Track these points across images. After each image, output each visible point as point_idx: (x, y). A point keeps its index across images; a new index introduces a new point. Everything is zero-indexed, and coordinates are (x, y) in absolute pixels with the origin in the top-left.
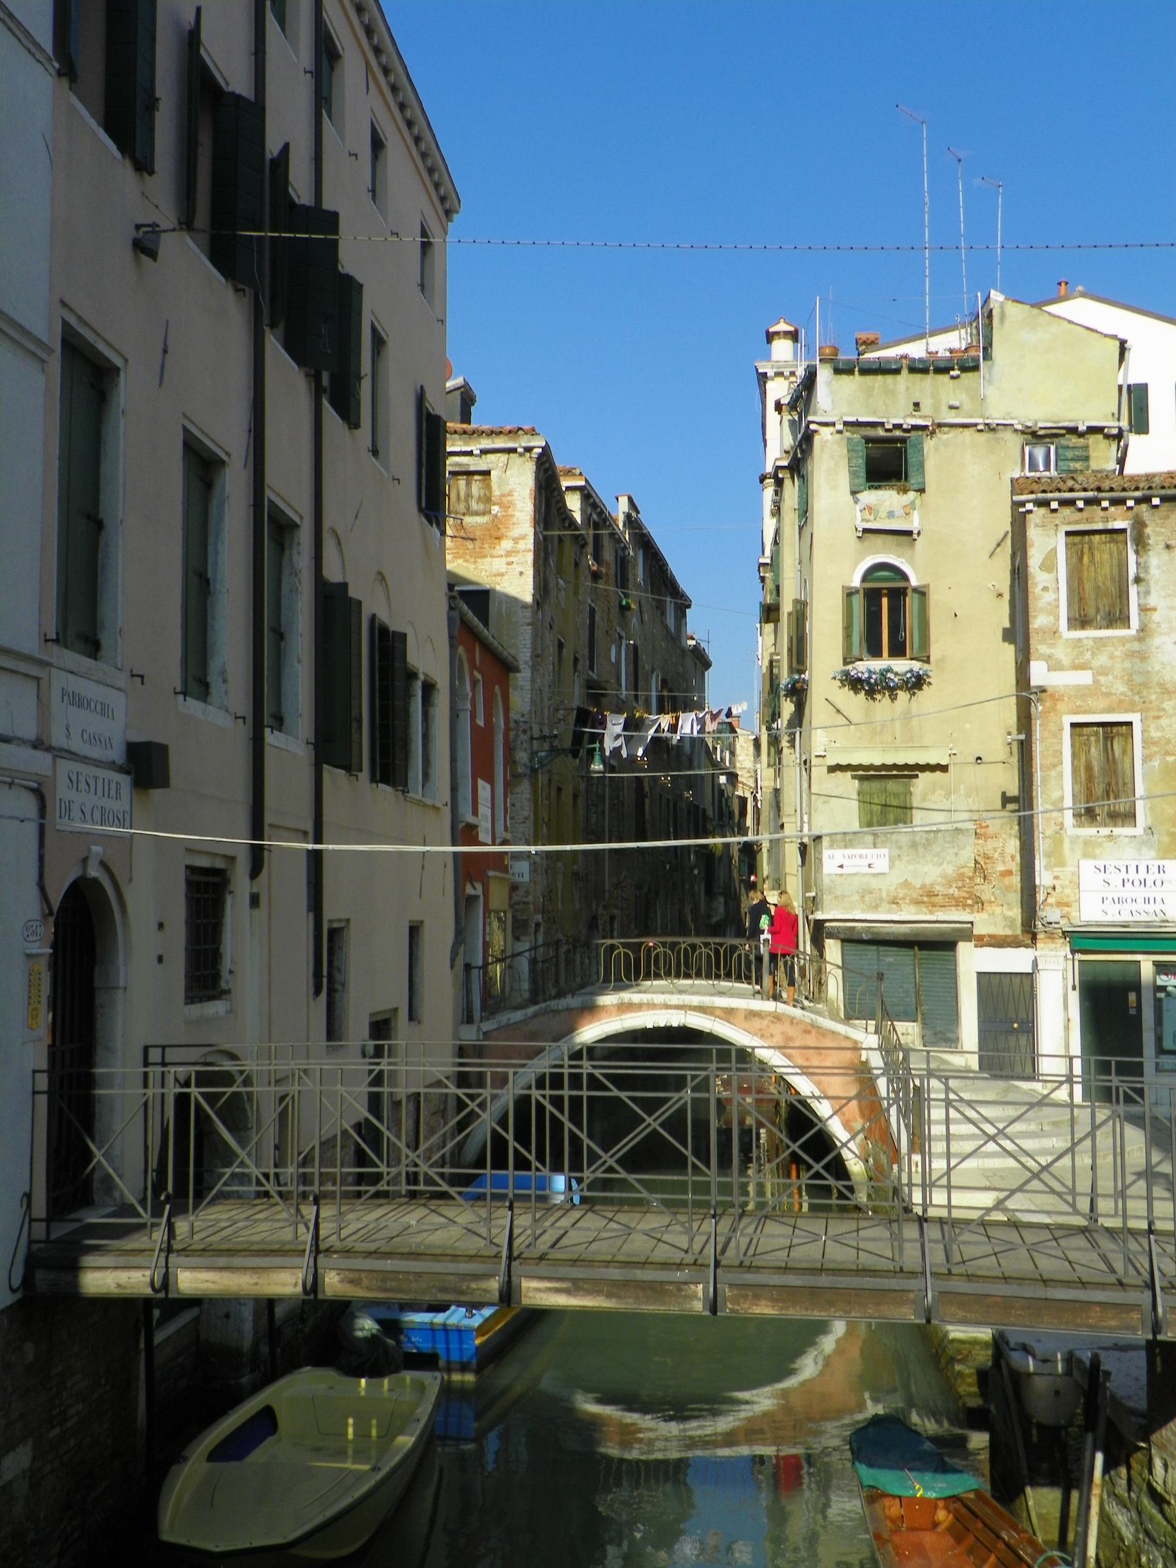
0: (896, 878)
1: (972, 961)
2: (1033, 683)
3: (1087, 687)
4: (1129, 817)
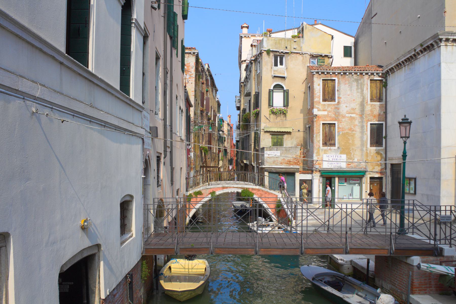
1: (299, 177)
2: (314, 114)
4: (334, 145)
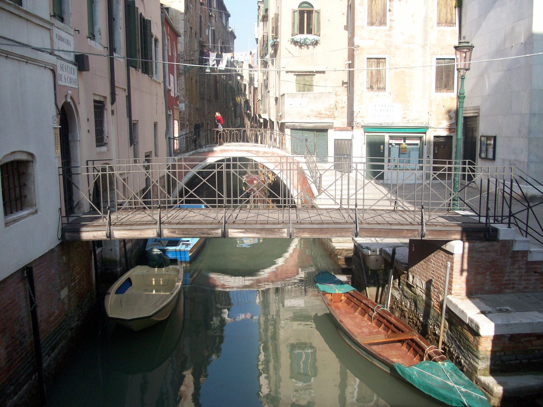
1: (332, 135)
2: (355, 44)
4: (384, 89)
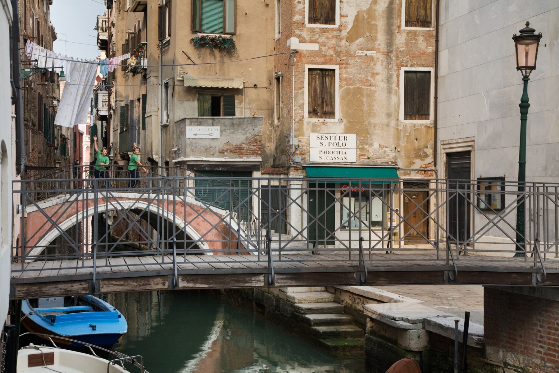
0: (224, 140)
1: (259, 181)
3: (317, 52)
4: (331, 114)
